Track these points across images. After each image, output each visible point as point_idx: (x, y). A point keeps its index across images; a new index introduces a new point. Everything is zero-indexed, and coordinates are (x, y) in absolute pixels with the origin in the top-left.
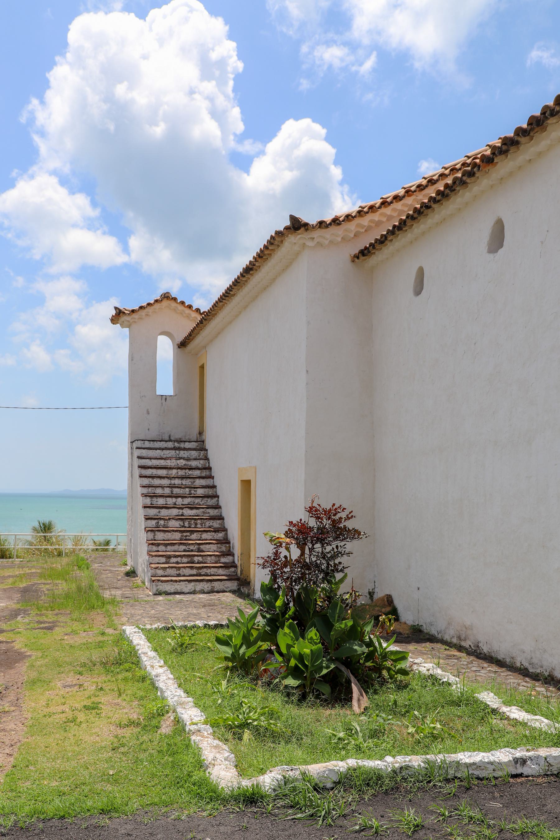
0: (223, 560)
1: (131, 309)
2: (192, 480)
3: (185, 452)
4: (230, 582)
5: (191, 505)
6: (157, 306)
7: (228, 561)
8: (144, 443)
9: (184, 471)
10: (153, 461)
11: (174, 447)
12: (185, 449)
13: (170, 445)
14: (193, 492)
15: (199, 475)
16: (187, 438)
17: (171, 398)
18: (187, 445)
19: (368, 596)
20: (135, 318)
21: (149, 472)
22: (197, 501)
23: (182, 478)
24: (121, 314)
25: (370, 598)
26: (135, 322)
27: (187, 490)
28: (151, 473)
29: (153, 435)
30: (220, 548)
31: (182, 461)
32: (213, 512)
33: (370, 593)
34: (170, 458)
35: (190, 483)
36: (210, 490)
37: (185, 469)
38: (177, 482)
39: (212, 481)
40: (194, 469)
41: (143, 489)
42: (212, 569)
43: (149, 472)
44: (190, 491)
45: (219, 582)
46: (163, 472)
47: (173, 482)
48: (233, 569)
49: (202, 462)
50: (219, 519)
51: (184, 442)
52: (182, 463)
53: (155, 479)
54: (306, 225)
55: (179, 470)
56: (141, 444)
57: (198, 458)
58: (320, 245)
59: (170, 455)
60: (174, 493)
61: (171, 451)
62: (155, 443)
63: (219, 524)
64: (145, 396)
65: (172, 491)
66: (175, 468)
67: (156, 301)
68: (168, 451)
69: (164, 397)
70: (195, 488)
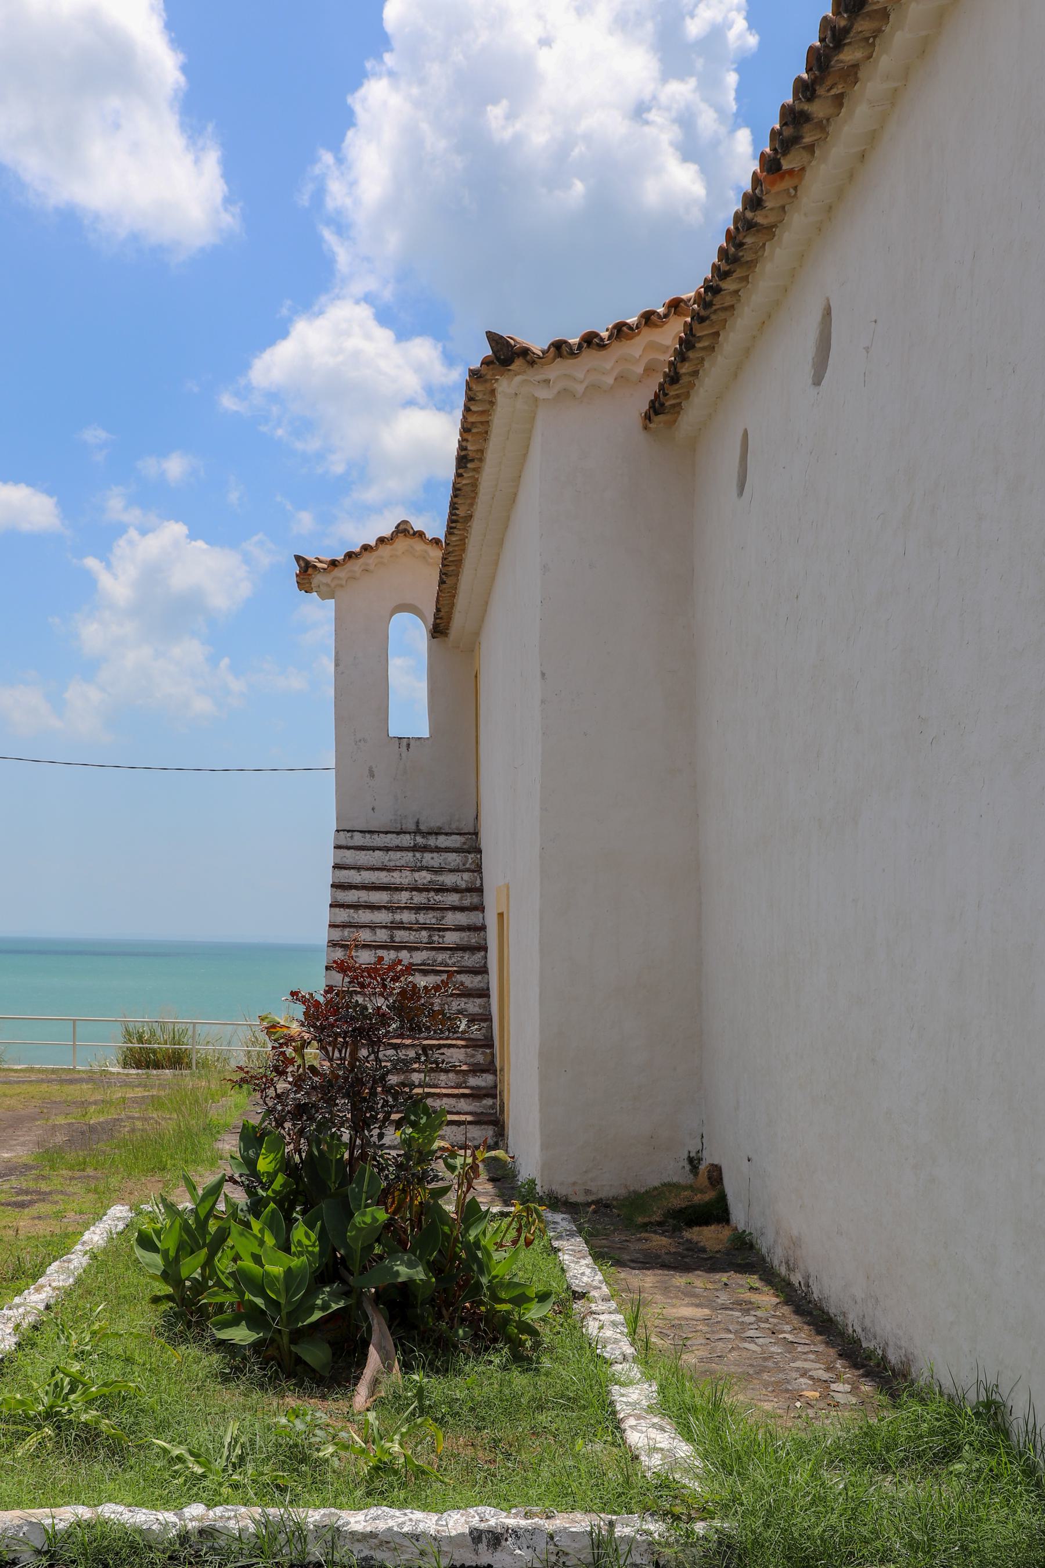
0: (473, 1081)
1: (329, 559)
2: (438, 914)
3: (435, 855)
4: (478, 1127)
5: (428, 965)
6: (385, 551)
7: (483, 1084)
8: (352, 837)
10: (363, 873)
11: (415, 845)
13: (406, 840)
14: (436, 938)
15: (457, 903)
16: (454, 826)
17: (418, 743)
18: (442, 841)
19: (688, 1167)
20: (339, 578)
21: (352, 896)
22: (441, 957)
23: (418, 909)
24: (310, 571)
25: (691, 1171)
26: (342, 586)
27: (424, 933)
28: (355, 899)
29: (383, 819)
30: (473, 1056)
31: (424, 873)
32: (470, 981)
33: (691, 1160)
34: (399, 869)
35: (434, 921)
36: (472, 934)
37: (428, 890)
38: (407, 917)
39: (481, 915)
40: (447, 890)
41: (332, 930)
42: (445, 1100)
43: (352, 896)
44: (430, 936)
45: (454, 1128)
46: (376, 897)
47: (398, 917)
48: (489, 1102)
49: (466, 876)
50: (480, 996)
53: (360, 912)
54: (525, 352)
55: (414, 893)
56: (351, 838)
57: (461, 867)
58: (565, 394)
59: (402, 862)
60: (397, 939)
61: (403, 854)
62: (375, 836)
63: (480, 1005)
64: (365, 741)
65: (392, 937)
66: (406, 889)
67: (381, 540)
68: (399, 854)
69: (405, 742)
70: (439, 930)
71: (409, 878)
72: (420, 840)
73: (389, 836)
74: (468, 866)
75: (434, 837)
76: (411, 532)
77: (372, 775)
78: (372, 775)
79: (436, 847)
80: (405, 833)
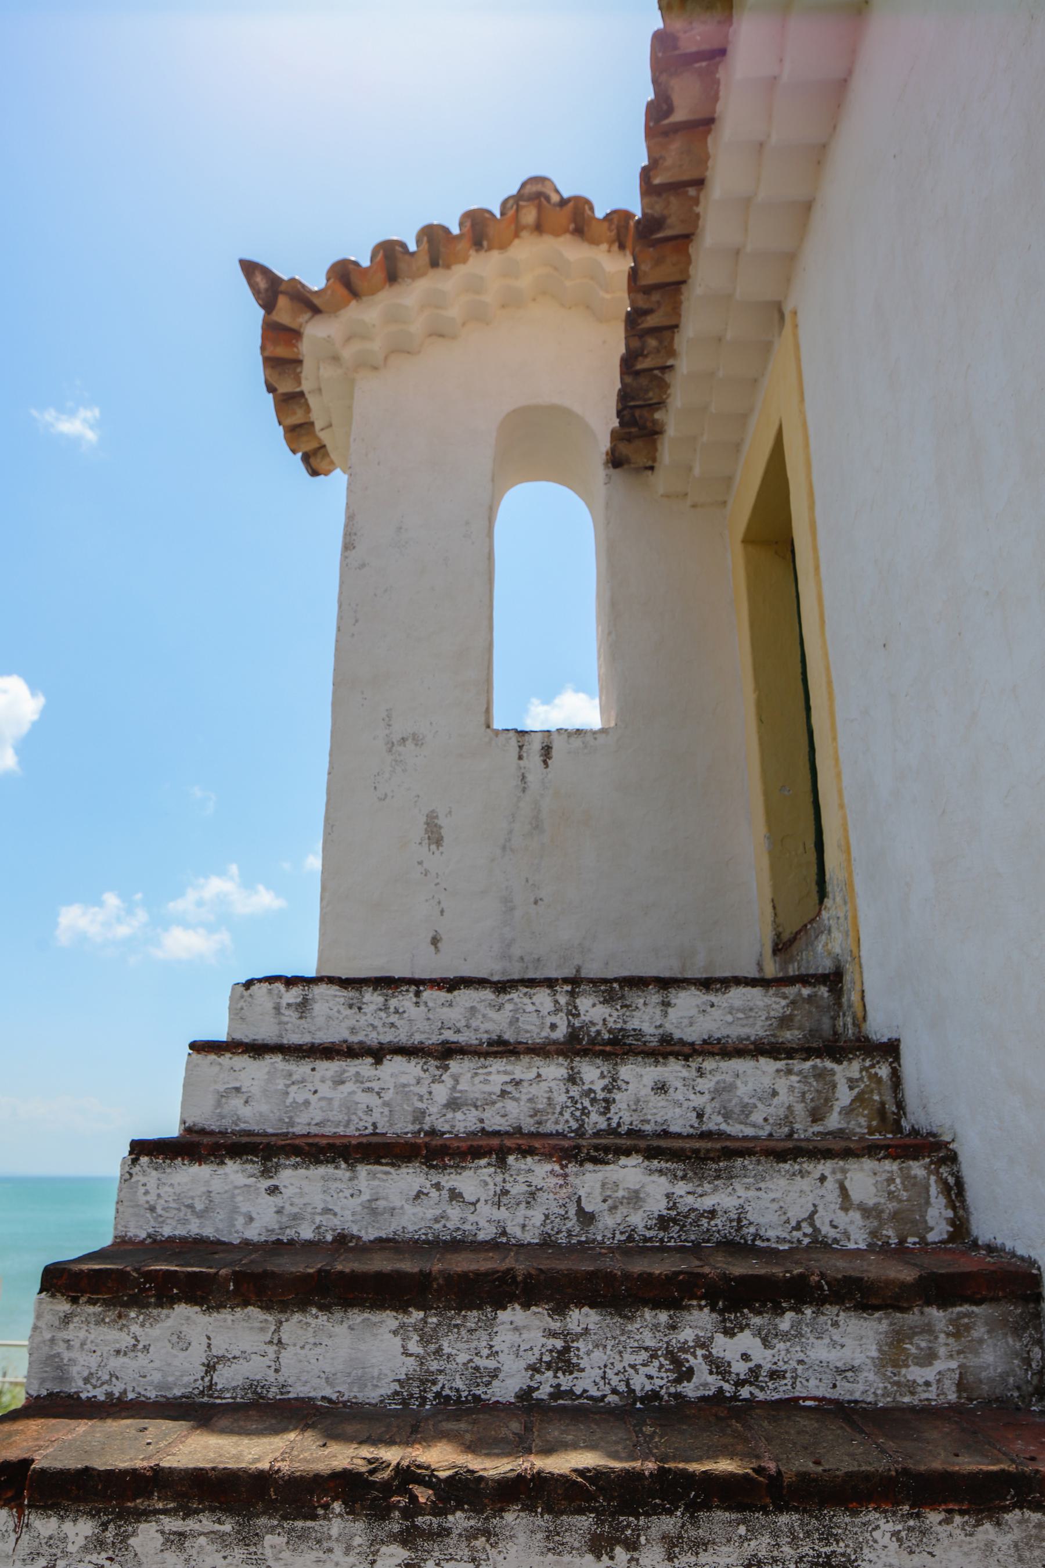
3: (673, 1071)
8: (303, 1007)
9: (648, 1326)
12: (667, 1048)
17: (576, 742)
31: (630, 1172)
34: (493, 1147)
37: (670, 1294)
49: (865, 1179)
51: (665, 984)
52: (631, 1195)
53: (147, 1537)
55: (580, 1318)
57: (805, 1129)
61: (522, 1069)
62: (405, 1000)
64: (418, 740)
68: (498, 1072)
69: (535, 745)
71: (548, 1203)
72: (594, 1011)
73: (465, 997)
74: (834, 1121)
75: (654, 997)
76: (555, 198)
77: (434, 836)
78: (434, 836)
79: (666, 1039)
80: (531, 983)
